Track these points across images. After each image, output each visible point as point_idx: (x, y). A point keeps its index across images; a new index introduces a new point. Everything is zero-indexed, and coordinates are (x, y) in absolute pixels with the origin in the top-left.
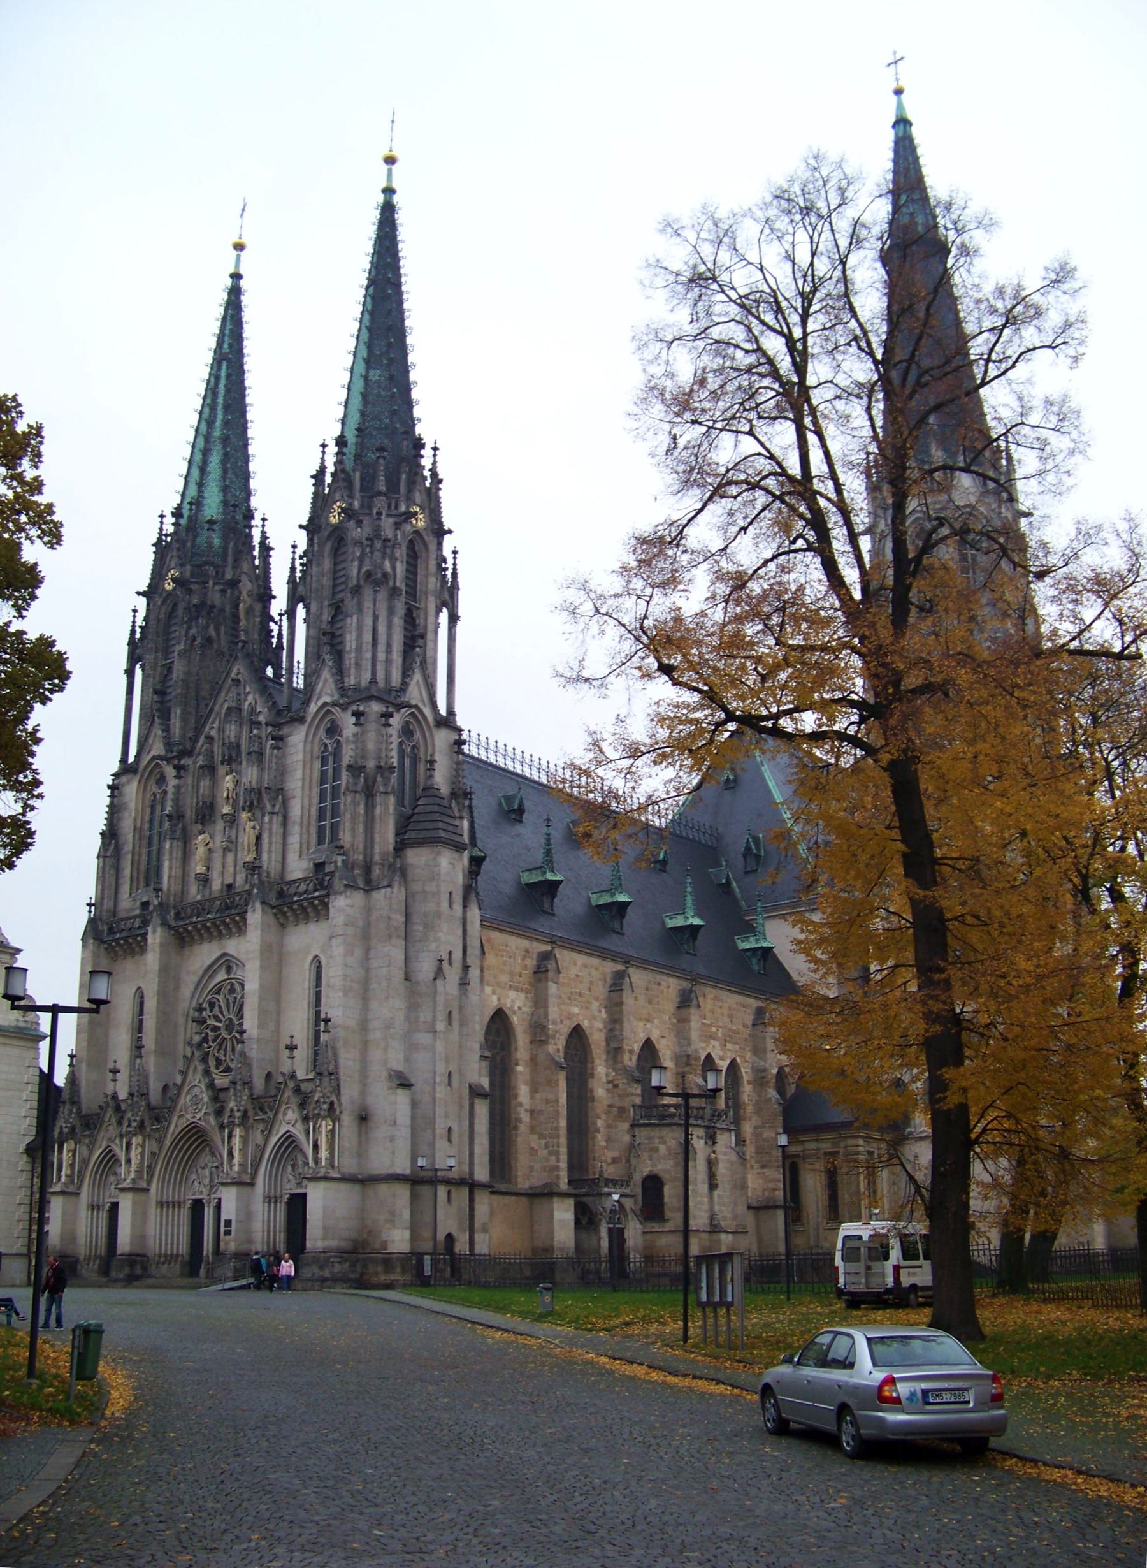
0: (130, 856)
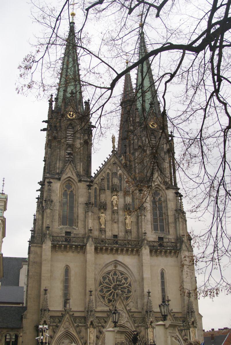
0: (58, 212)
